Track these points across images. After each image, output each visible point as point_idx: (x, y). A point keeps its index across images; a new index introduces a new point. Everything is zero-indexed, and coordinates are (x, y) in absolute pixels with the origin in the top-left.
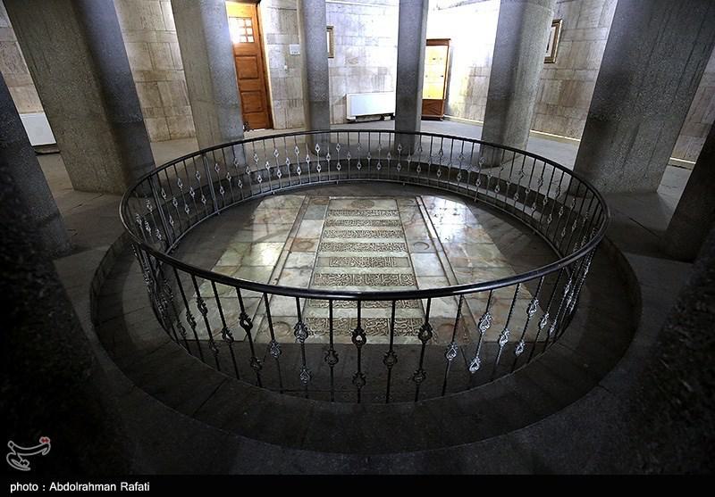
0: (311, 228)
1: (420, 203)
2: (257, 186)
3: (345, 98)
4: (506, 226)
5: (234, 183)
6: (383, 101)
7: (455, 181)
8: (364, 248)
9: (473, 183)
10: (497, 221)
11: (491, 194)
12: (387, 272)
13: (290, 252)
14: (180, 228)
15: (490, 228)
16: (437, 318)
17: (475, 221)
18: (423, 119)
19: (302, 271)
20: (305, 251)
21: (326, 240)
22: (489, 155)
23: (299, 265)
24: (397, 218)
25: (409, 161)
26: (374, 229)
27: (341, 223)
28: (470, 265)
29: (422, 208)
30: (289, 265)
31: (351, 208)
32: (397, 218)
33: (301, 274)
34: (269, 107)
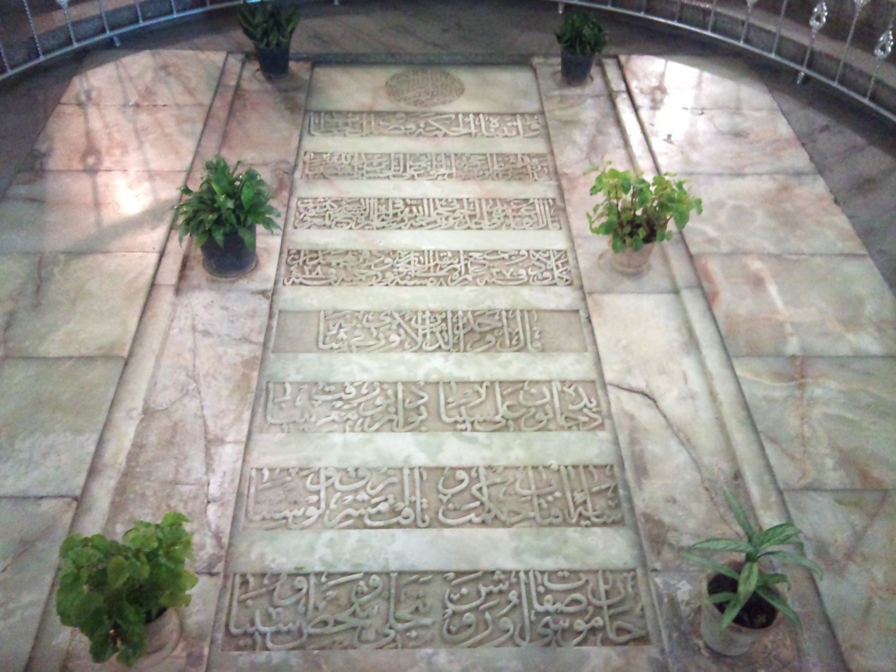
1: (617, 85)
8: (441, 269)
24: (539, 146)
26: (469, 190)
28: (793, 346)
31: (384, 104)
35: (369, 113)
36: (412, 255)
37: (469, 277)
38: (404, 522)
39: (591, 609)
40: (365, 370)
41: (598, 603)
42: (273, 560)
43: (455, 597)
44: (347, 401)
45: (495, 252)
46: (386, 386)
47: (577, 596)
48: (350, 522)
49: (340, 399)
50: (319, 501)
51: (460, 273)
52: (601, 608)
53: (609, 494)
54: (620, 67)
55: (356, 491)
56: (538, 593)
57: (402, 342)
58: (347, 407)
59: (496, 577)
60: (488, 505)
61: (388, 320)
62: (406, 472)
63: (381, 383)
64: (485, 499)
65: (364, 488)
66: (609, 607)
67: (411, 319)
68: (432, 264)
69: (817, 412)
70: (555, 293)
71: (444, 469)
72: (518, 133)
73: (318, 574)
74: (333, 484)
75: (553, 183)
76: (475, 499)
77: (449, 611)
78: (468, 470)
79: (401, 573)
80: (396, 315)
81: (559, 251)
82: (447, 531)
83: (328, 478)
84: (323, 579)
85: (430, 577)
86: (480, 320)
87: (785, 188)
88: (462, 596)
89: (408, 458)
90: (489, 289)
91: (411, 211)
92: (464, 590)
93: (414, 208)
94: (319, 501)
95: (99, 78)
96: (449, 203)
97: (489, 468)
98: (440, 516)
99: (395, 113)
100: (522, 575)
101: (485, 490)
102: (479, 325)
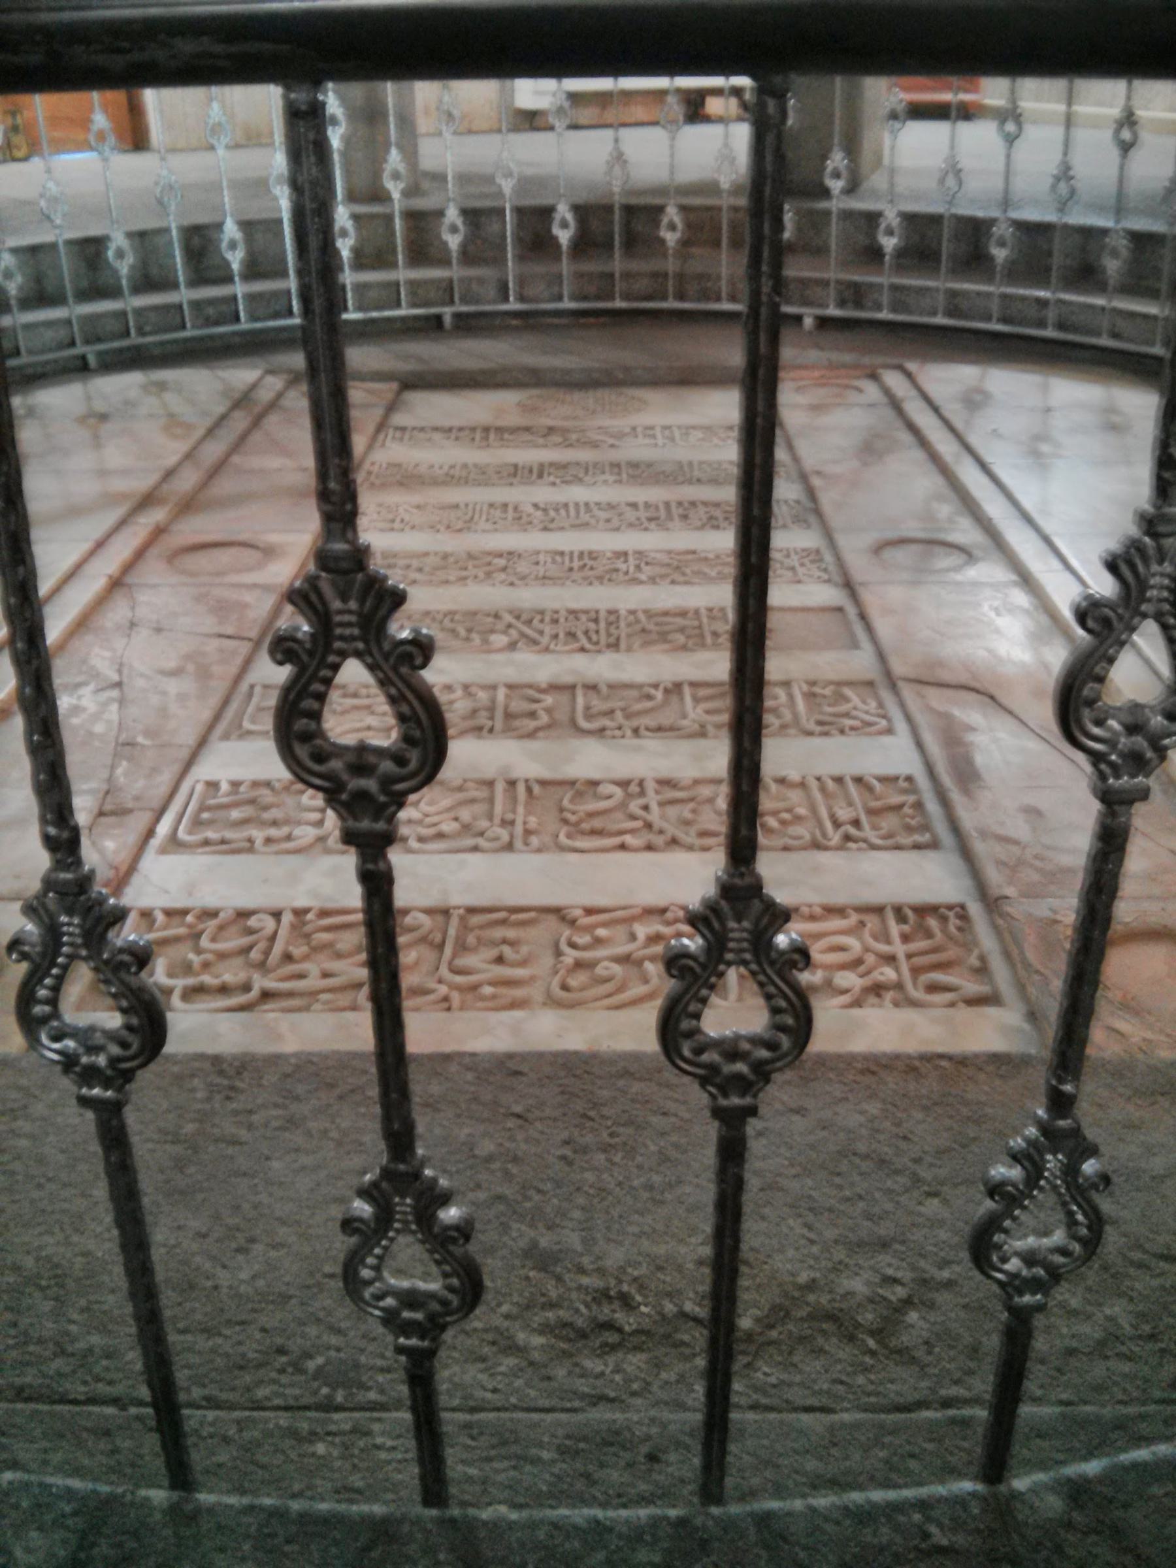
45: (694, 552)
51: (627, 573)
59: (669, 915)
62: (500, 787)
71: (572, 783)
76: (633, 818)
79: (472, 910)
85: (533, 914)
92: (601, 932)
96: (611, 506)
98: (562, 838)
101: (654, 807)
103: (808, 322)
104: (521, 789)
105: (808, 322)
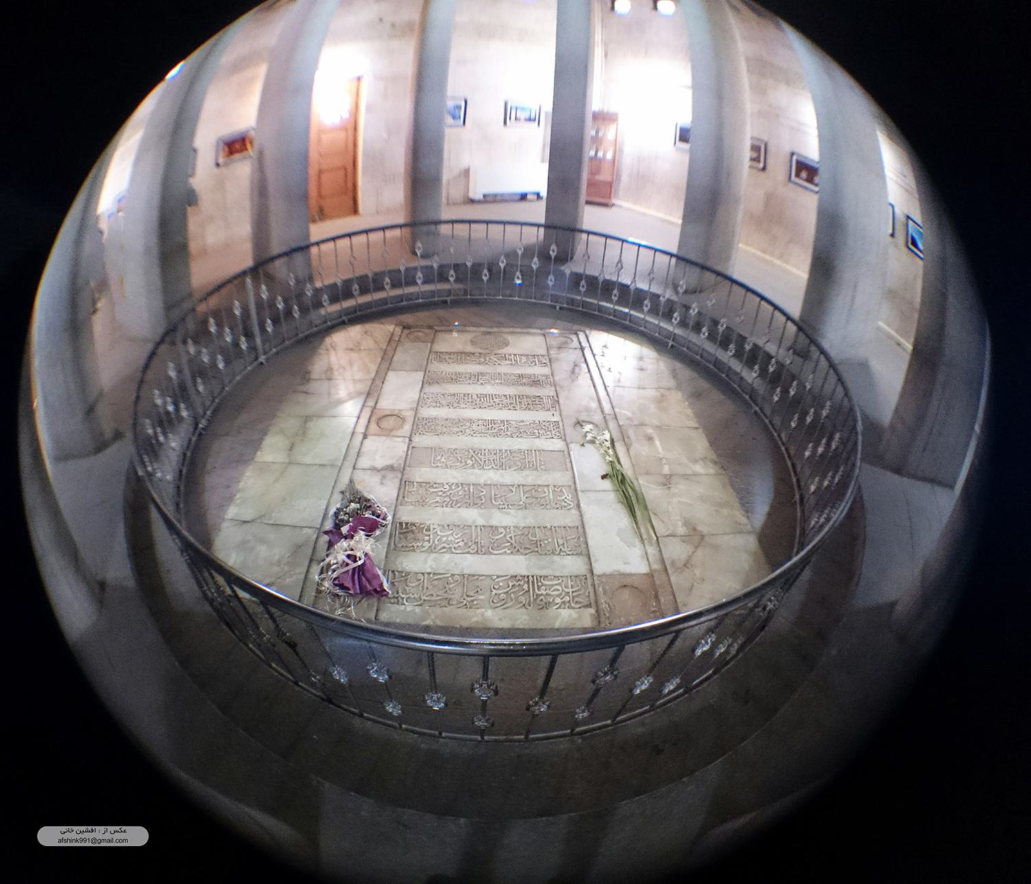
0: (401, 391)
1: (585, 344)
2: (322, 311)
3: (467, 172)
4: (717, 395)
5: (288, 312)
6: (533, 175)
7: (642, 311)
9: (668, 316)
10: (704, 384)
11: (693, 338)
12: (530, 480)
13: (365, 436)
14: (212, 392)
15: (696, 396)
16: (611, 576)
17: (672, 383)
18: (588, 203)
19: (384, 477)
20: (388, 433)
21: (427, 412)
22: (689, 278)
23: (380, 463)
25: (568, 272)
27: (455, 378)
28: (666, 470)
29: (588, 353)
30: (364, 462)
31: (470, 349)
32: (547, 371)
33: (382, 484)
34: (355, 186)
35: (461, 353)
36: (480, 421)
37: (509, 434)
38: (471, 551)
39: (564, 593)
40: (454, 477)
41: (566, 590)
42: (407, 566)
43: (496, 587)
44: (444, 492)
46: (464, 486)
47: (558, 587)
48: (445, 550)
49: (441, 491)
50: (430, 539)
52: (569, 593)
53: (576, 540)
54: (587, 336)
55: (448, 536)
56: (538, 586)
57: (473, 464)
58: (444, 495)
60: (514, 544)
61: (467, 453)
63: (462, 484)
64: (513, 542)
65: (452, 534)
66: (573, 592)
67: (478, 453)
68: (490, 426)
69: (675, 500)
70: (552, 442)
72: (536, 364)
73: (429, 574)
74: (436, 532)
75: (553, 389)
76: (509, 542)
77: (493, 593)
78: (505, 528)
80: (471, 451)
81: (555, 422)
82: (493, 556)
83: (434, 529)
84: (431, 576)
86: (514, 454)
87: (662, 395)
88: (500, 586)
89: (474, 521)
90: (519, 439)
91: (480, 400)
92: (501, 584)
93: (482, 399)
94: (430, 539)
95: (339, 339)
97: (516, 527)
99: (473, 354)
100: (530, 577)
102: (513, 457)
103: (558, 308)
104: (479, 528)
105: (558, 308)
